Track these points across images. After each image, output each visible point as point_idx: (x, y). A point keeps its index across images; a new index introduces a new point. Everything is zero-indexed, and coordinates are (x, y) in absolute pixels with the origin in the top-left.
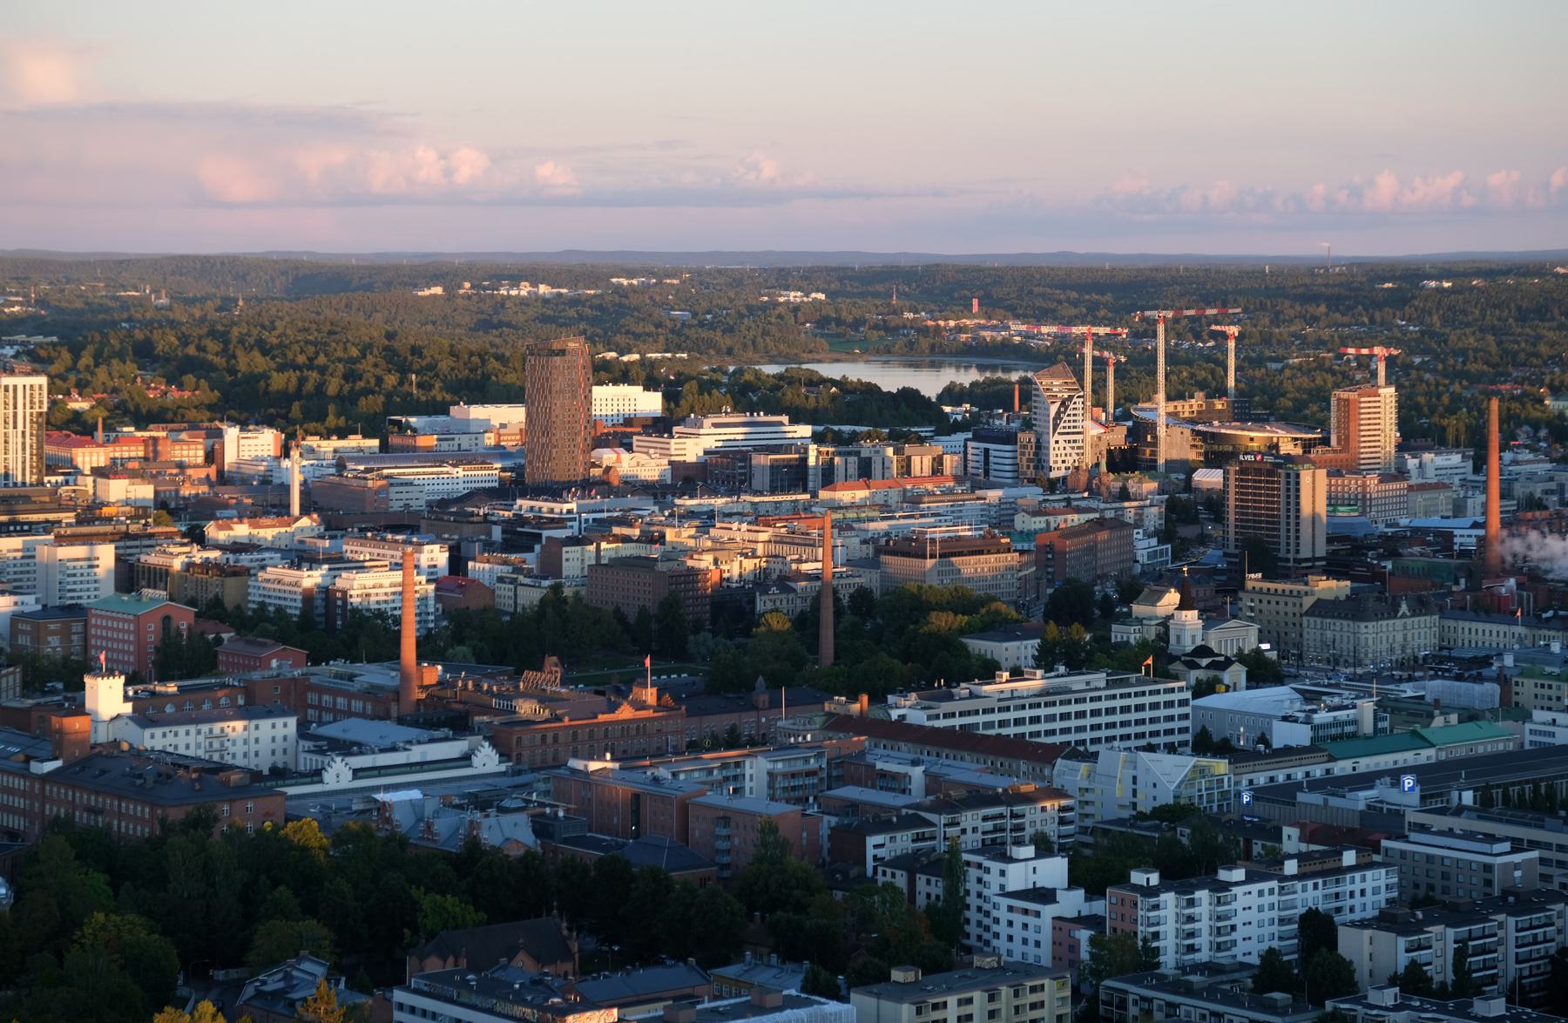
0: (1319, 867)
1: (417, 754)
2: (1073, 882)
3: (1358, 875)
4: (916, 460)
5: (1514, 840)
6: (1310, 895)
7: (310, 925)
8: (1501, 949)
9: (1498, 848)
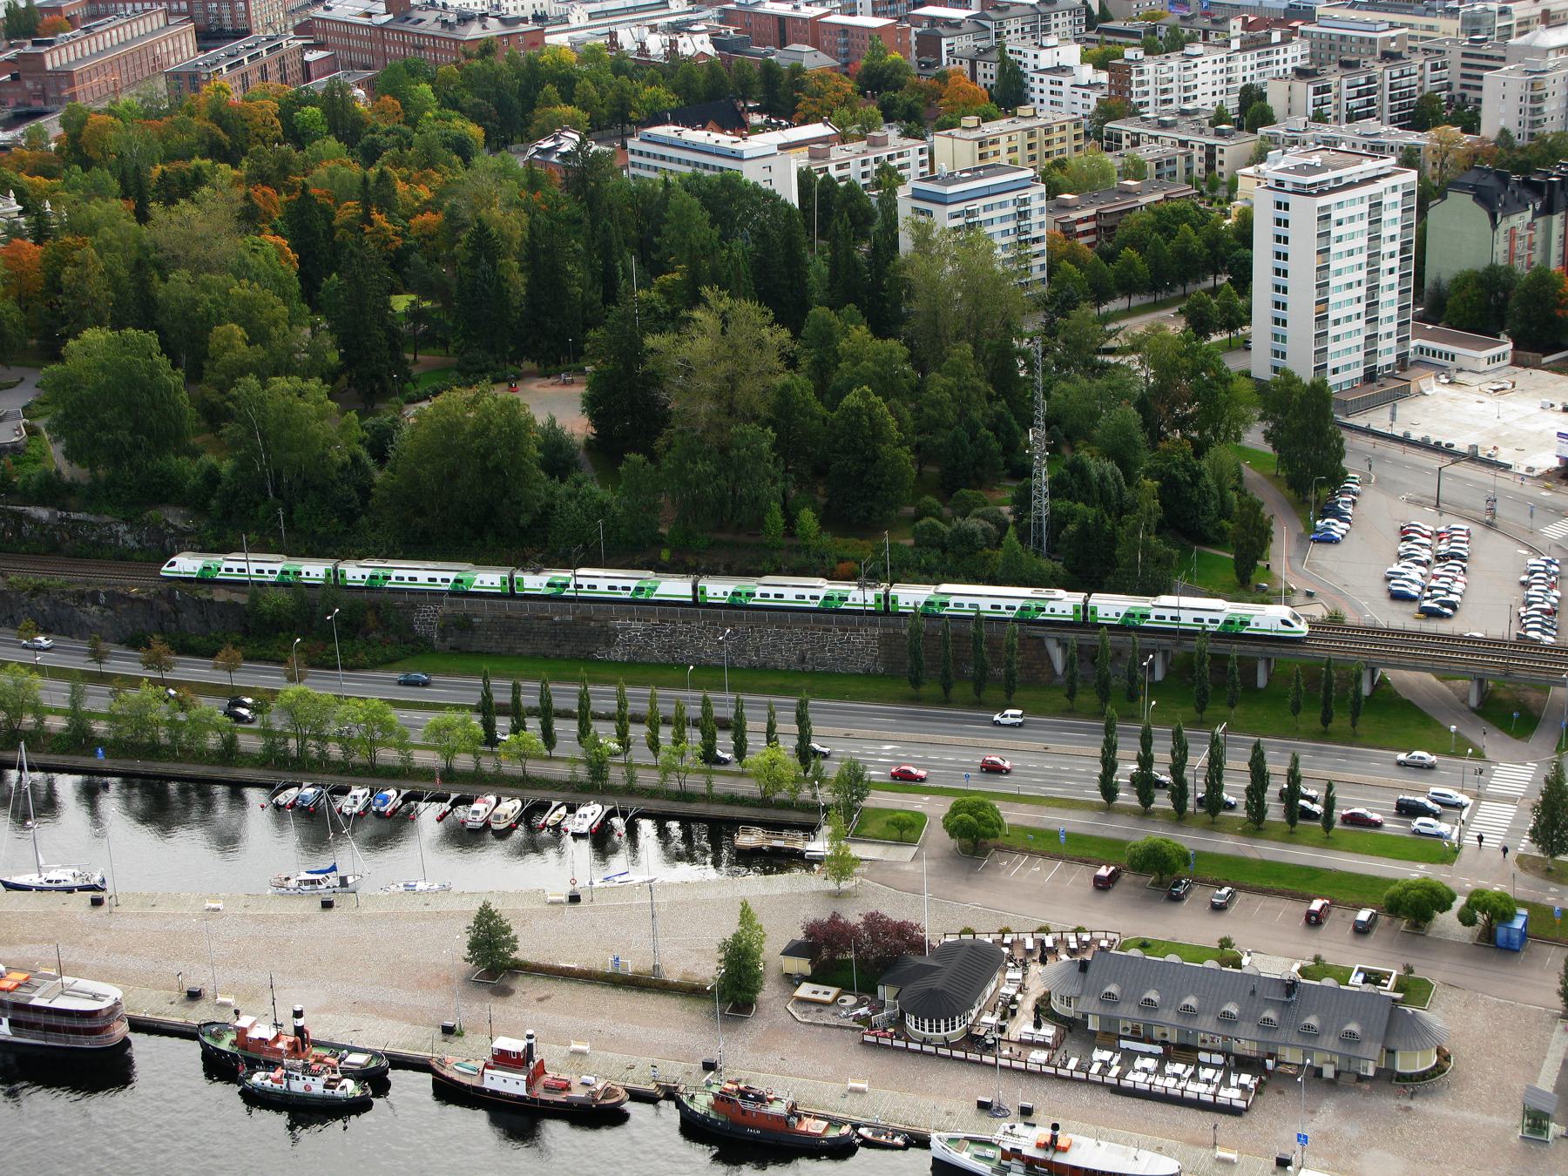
2: (1084, 60)
5: (1391, 23)
6: (1245, 67)
7: (570, 110)
8: (1379, 92)
9: (1379, 27)
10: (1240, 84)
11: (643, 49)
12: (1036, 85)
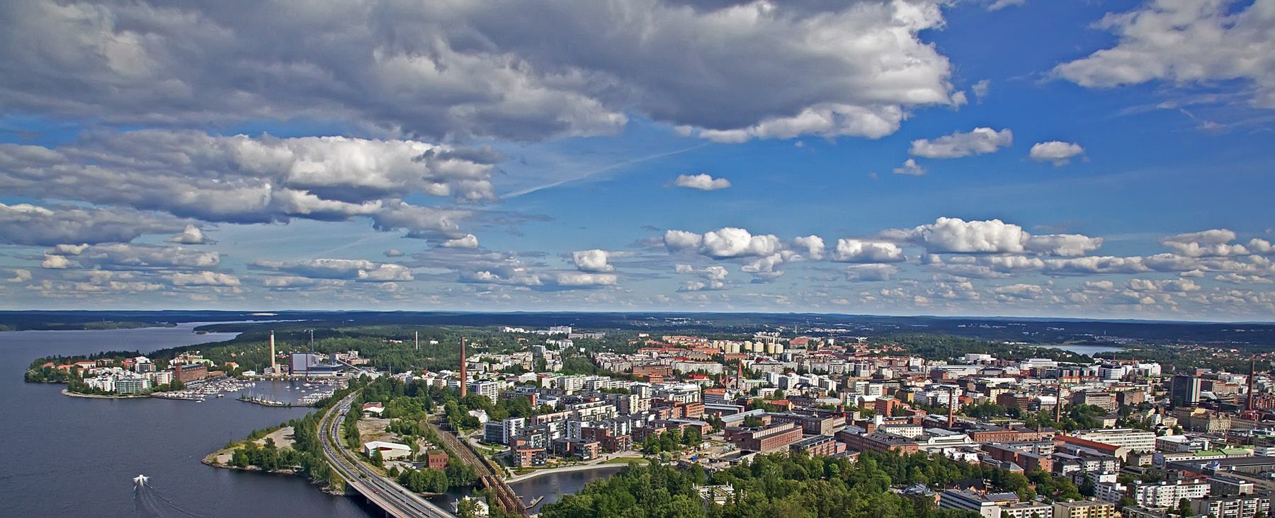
0: (1188, 482)
1: (950, 438)
3: (1198, 486)
4: (1085, 372)
6: (1183, 492)
10: (1181, 497)
11: (952, 457)
12: (1098, 488)
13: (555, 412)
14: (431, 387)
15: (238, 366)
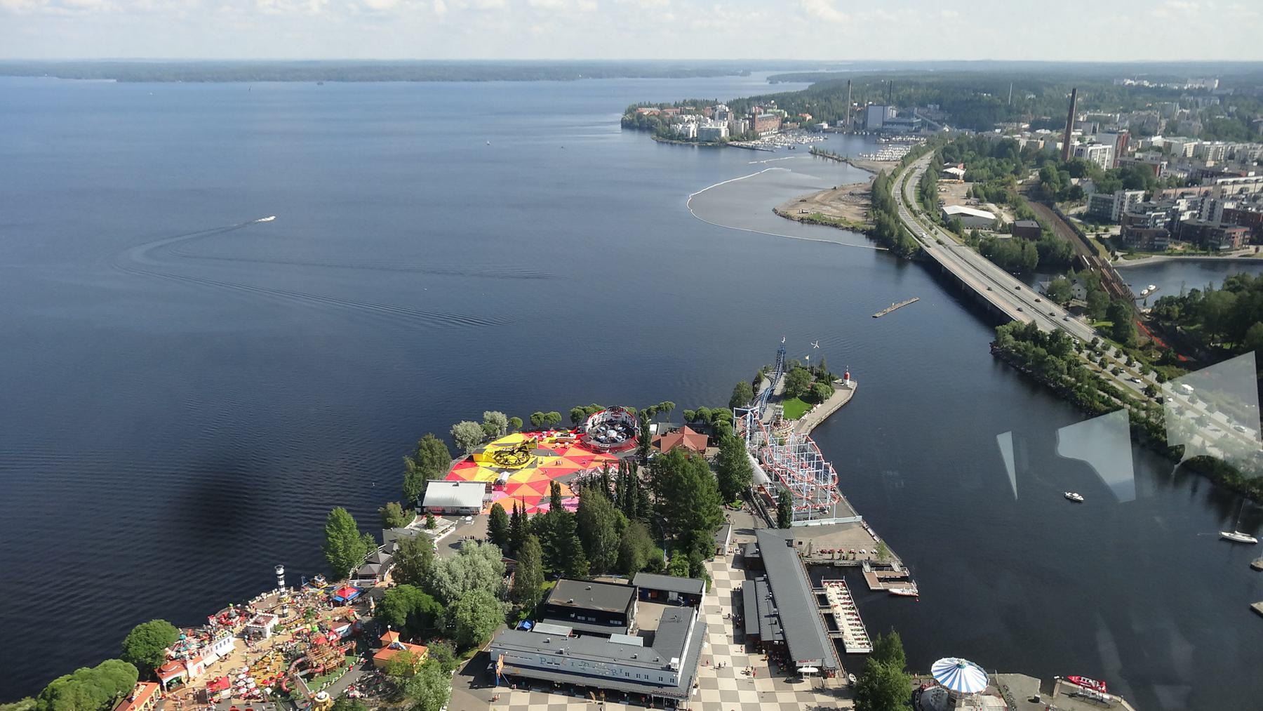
13: (1187, 186)
14: (1025, 149)
15: (811, 117)
